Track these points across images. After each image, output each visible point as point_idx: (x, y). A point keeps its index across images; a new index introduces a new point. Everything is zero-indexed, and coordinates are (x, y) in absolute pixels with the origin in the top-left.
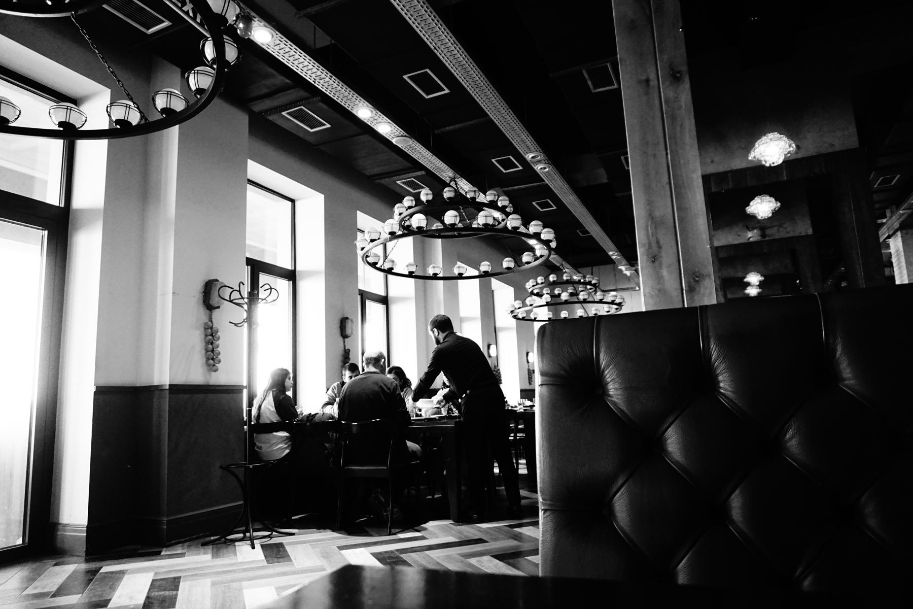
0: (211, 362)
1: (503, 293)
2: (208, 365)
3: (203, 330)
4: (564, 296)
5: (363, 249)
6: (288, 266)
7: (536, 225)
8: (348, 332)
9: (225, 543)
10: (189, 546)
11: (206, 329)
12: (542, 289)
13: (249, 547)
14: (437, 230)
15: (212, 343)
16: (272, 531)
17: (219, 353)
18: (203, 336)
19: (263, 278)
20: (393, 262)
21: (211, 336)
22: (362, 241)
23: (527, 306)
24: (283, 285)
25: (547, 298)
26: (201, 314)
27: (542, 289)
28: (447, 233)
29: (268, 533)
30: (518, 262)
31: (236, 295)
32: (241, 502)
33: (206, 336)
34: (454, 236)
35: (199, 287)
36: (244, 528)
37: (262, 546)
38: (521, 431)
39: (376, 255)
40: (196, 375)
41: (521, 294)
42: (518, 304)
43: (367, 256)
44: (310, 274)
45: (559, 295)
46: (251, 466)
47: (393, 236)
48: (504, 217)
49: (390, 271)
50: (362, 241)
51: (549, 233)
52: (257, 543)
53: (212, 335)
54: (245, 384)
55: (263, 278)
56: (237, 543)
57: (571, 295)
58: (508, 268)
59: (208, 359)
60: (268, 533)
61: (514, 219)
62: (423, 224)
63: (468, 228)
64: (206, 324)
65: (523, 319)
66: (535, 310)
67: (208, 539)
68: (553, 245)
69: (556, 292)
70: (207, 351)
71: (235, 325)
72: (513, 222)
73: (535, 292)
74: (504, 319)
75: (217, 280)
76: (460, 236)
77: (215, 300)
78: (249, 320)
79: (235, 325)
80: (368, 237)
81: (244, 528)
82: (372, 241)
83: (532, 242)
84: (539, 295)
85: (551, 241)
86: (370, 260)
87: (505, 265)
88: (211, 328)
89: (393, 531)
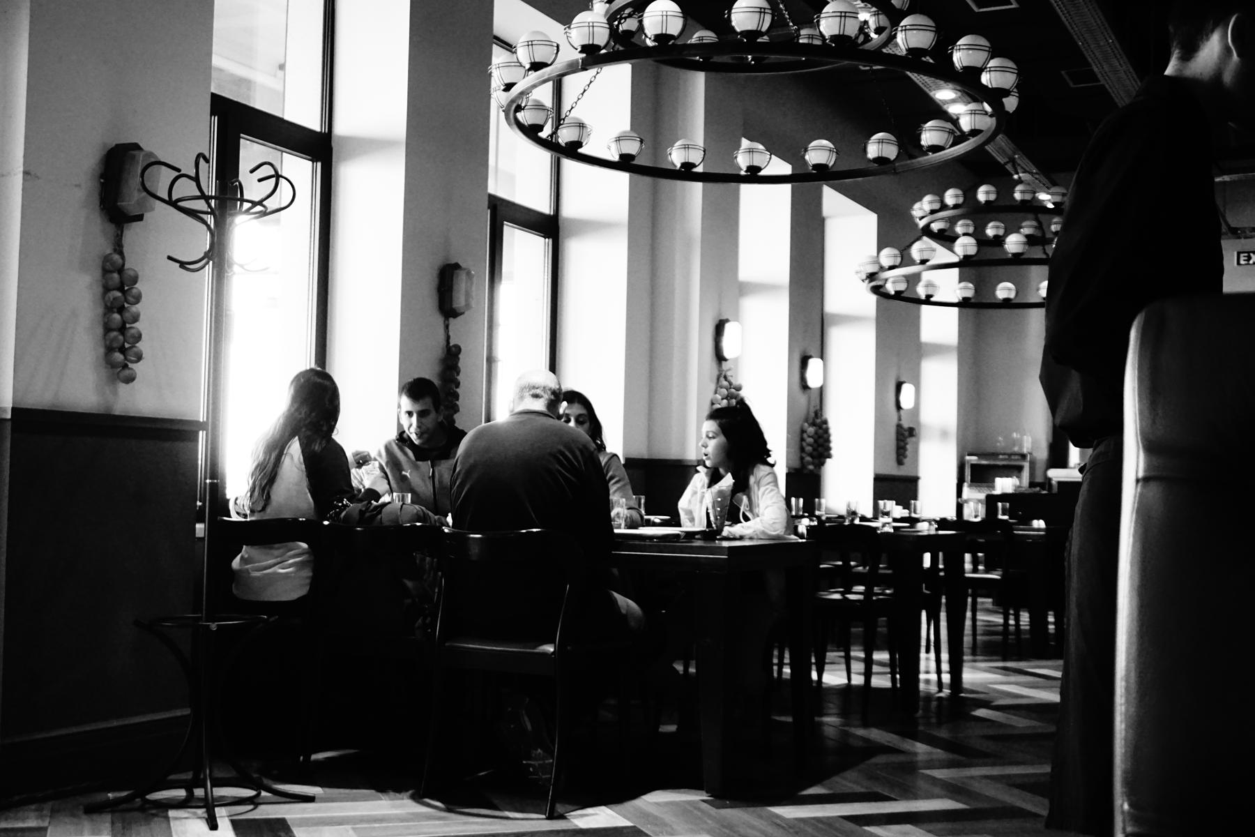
0: (119, 357)
1: (851, 228)
2: (111, 364)
3: (98, 273)
4: (1014, 243)
5: (508, 87)
6: (313, 122)
7: (971, 47)
8: (459, 301)
9: (142, 809)
10: (54, 813)
11: (105, 272)
12: (952, 221)
13: (202, 826)
14: (700, 47)
15: (121, 310)
16: (258, 787)
17: (139, 337)
18: (100, 290)
19: (251, 152)
20: (581, 126)
21: (118, 292)
22: (508, 65)
23: (912, 262)
24: (299, 169)
25: (965, 246)
26: (97, 237)
27: (952, 221)
28: (727, 56)
29: (249, 793)
30: (909, 143)
31: (185, 188)
32: (187, 712)
33: (107, 289)
34: (747, 68)
35: (87, 161)
36: (188, 776)
37: (236, 825)
38: (884, 581)
39: (539, 106)
40: (79, 387)
41: (898, 232)
42: (888, 256)
43: (519, 108)
44: (368, 146)
45: (999, 241)
46: (214, 626)
47: (593, 56)
48: (884, 20)
49: (572, 151)
50: (508, 65)
51: (1002, 69)
52: (221, 812)
53: (121, 289)
54: (202, 417)
55: (251, 152)
56: (172, 813)
57: (1031, 240)
58: (881, 160)
59: (109, 350)
60: (249, 793)
61: (914, 27)
62: (675, 27)
63: (790, 43)
64: (106, 259)
65: (898, 295)
66: (927, 276)
67: (99, 797)
68: (1011, 103)
69: (990, 232)
70: (107, 329)
71: (183, 265)
72: (912, 35)
73: (935, 227)
74: (846, 292)
75: (136, 147)
76: (760, 66)
77: (131, 198)
78: (217, 254)
79: (183, 265)
80: (524, 56)
81: (188, 776)
82: (536, 66)
83: (944, 94)
84: (946, 238)
85: (1006, 93)
86: (525, 117)
87: (873, 151)
88: (121, 270)
89: (560, 808)
